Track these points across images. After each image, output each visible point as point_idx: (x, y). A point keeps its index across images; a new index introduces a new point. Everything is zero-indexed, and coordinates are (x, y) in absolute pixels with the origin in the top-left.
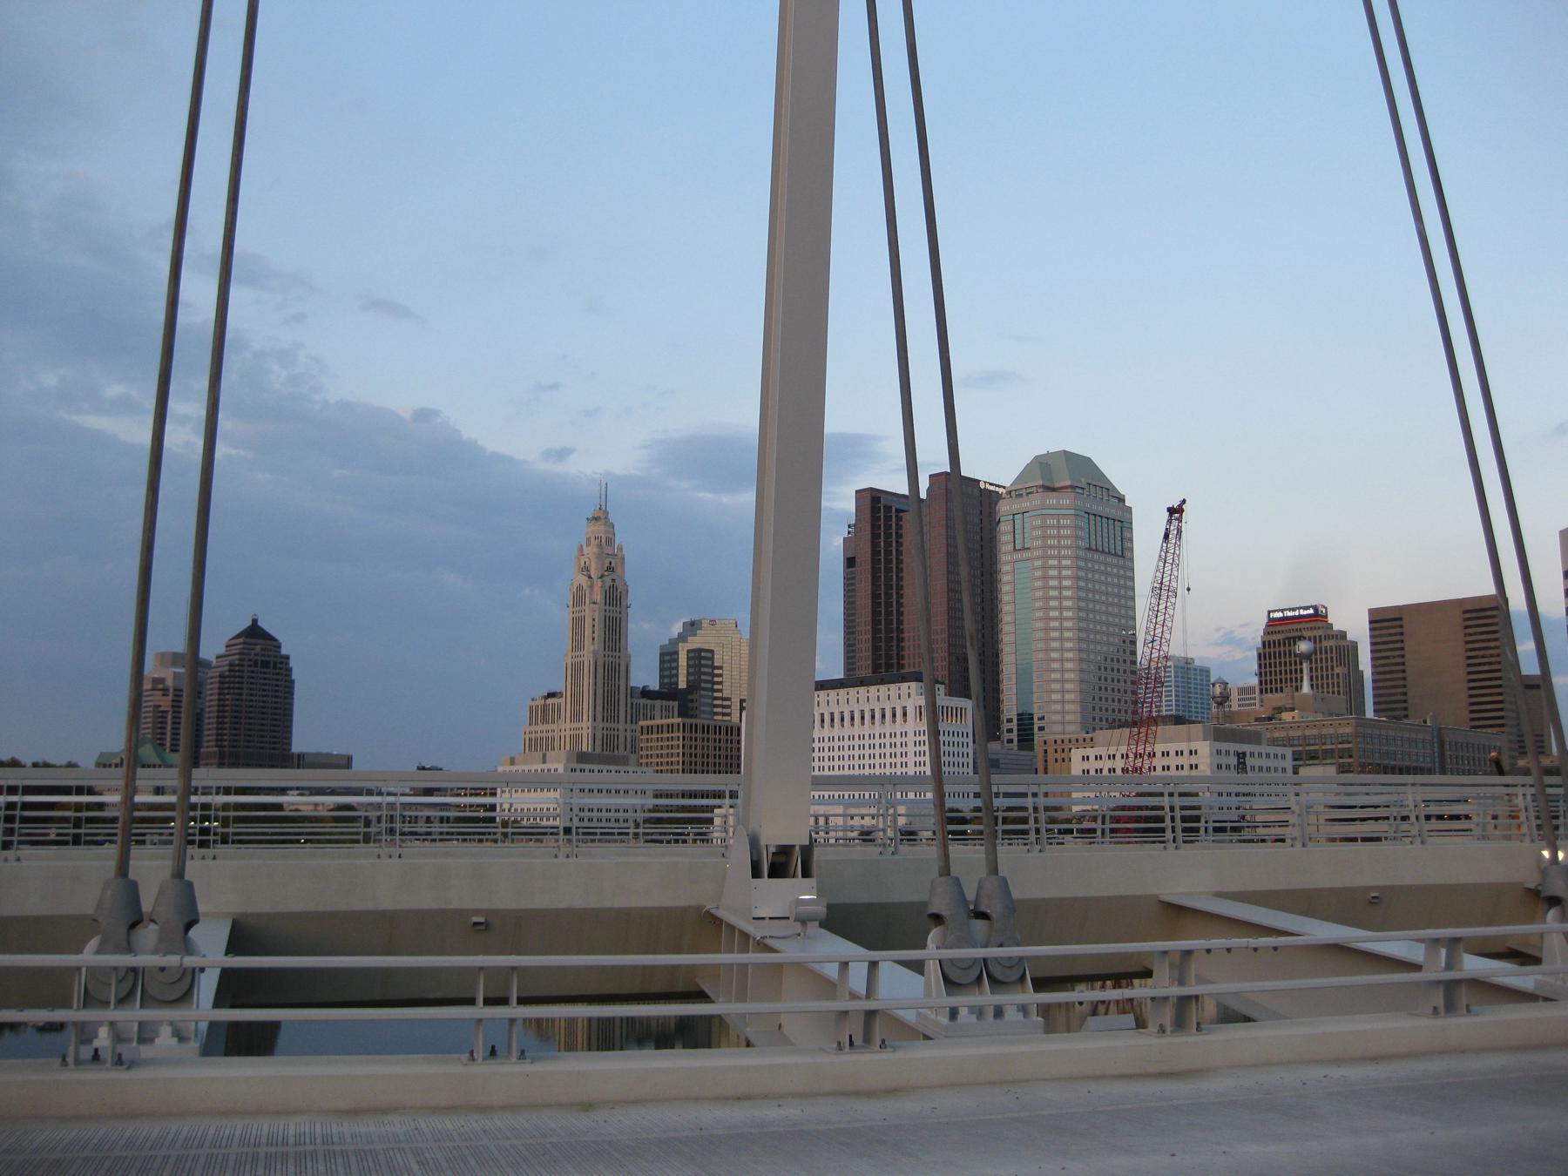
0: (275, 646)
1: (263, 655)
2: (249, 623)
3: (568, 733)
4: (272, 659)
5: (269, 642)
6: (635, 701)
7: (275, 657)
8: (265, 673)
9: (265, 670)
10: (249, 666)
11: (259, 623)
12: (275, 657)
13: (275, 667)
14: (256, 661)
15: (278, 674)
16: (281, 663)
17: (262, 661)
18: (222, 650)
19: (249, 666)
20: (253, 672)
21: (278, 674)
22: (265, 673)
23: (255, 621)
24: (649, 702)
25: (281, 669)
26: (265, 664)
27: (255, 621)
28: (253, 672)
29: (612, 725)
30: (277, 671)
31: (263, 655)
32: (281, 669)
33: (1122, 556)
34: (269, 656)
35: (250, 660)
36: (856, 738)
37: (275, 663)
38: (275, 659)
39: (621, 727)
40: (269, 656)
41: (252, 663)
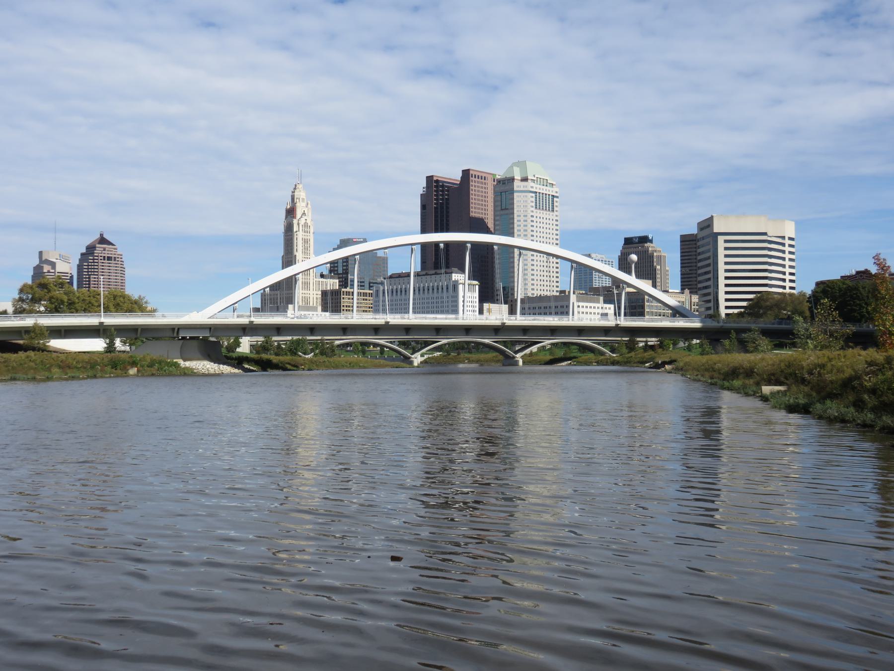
0: (115, 249)
1: (108, 254)
2: (99, 236)
3: (285, 295)
4: (113, 256)
5: (111, 246)
6: (317, 280)
7: (115, 254)
8: (110, 263)
9: (110, 262)
10: (101, 260)
11: (104, 236)
12: (115, 254)
13: (115, 260)
14: (104, 257)
15: (116, 264)
16: (118, 258)
17: (108, 257)
18: (84, 251)
19: (101, 260)
20: (103, 263)
21: (116, 264)
22: (110, 263)
23: (101, 235)
24: (324, 280)
25: (118, 261)
26: (109, 258)
27: (101, 235)
28: (103, 263)
29: (305, 292)
30: (116, 262)
31: (108, 254)
32: (118, 261)
33: (553, 211)
34: (111, 254)
35: (101, 256)
36: (426, 299)
37: (115, 258)
38: (115, 256)
39: (311, 292)
40: (111, 254)
41: (102, 258)
